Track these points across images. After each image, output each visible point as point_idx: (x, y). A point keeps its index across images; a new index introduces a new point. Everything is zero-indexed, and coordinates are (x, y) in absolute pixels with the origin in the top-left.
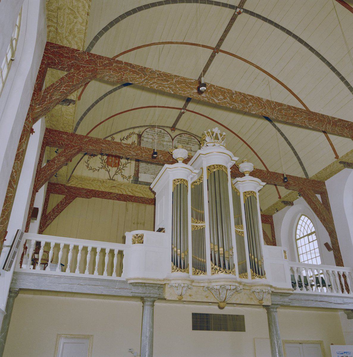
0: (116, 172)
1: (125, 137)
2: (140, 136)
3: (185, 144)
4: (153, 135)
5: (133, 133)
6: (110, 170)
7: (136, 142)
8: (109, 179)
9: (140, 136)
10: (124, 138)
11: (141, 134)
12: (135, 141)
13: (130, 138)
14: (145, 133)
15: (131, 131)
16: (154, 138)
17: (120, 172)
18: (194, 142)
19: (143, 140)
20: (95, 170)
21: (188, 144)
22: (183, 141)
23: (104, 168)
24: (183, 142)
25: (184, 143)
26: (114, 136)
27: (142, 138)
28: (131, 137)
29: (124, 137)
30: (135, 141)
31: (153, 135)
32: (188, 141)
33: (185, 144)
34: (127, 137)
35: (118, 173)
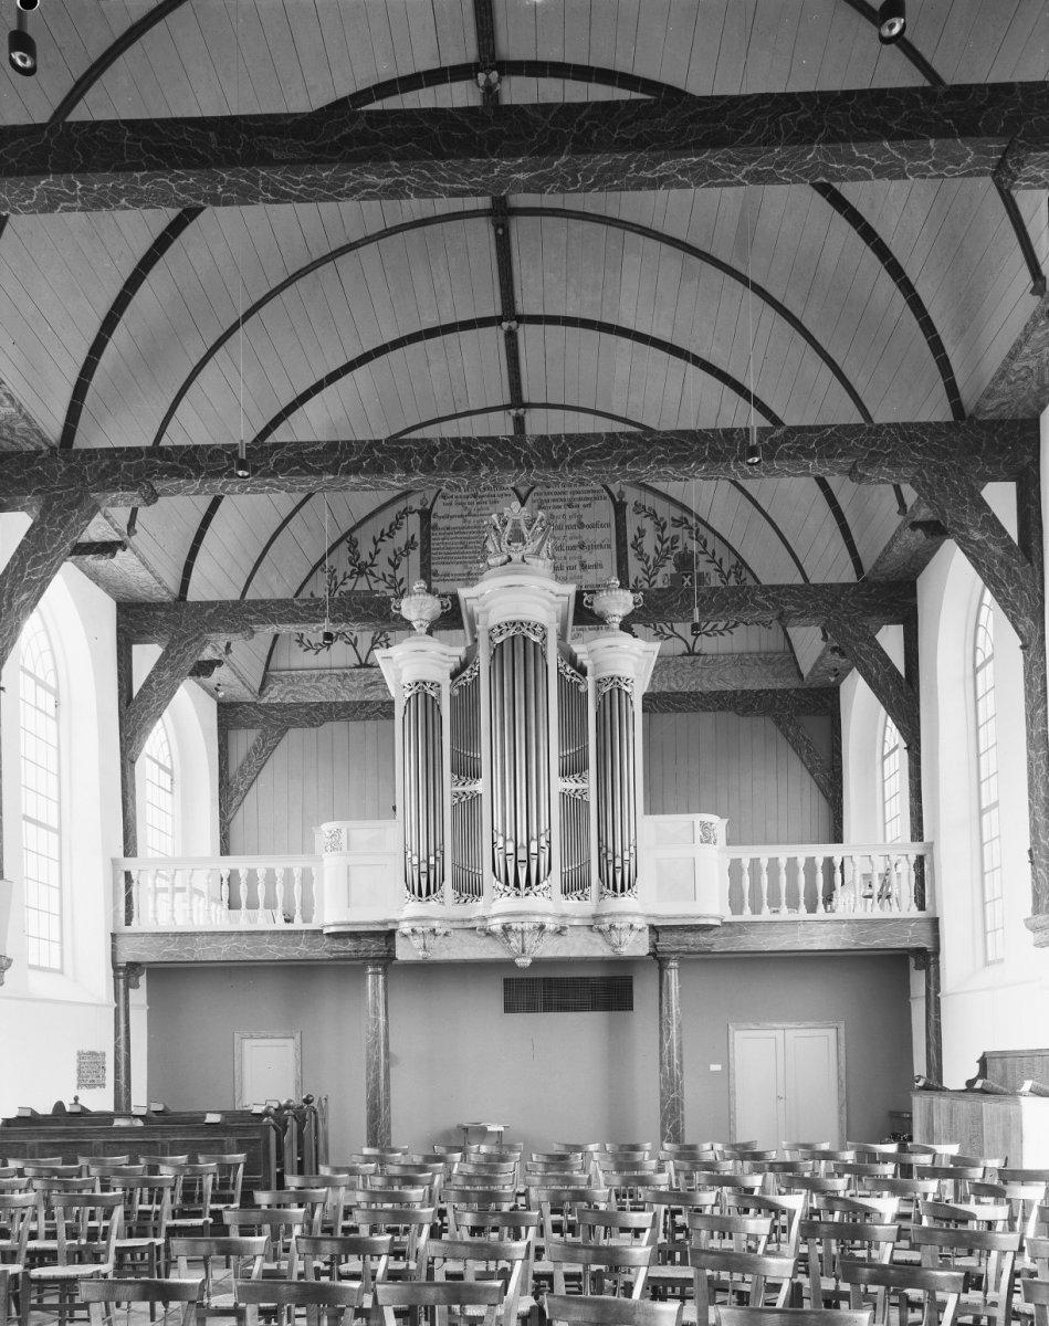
0: (374, 642)
1: (387, 531)
2: (426, 515)
3: (560, 507)
4: (462, 504)
5: (407, 511)
6: (356, 638)
7: (417, 539)
8: (357, 667)
9: (426, 515)
10: (382, 535)
11: (428, 507)
12: (413, 537)
13: (399, 529)
14: (440, 501)
15: (400, 506)
16: (466, 513)
17: (383, 639)
18: (591, 495)
19: (436, 527)
20: (319, 647)
21: (570, 506)
22: (554, 500)
23: (342, 639)
24: (556, 504)
25: (560, 504)
26: (355, 535)
27: (433, 521)
28: (402, 524)
29: (382, 532)
30: (413, 537)
31: (462, 504)
32: (569, 496)
33: (560, 507)
34: (391, 526)
35: (378, 645)
